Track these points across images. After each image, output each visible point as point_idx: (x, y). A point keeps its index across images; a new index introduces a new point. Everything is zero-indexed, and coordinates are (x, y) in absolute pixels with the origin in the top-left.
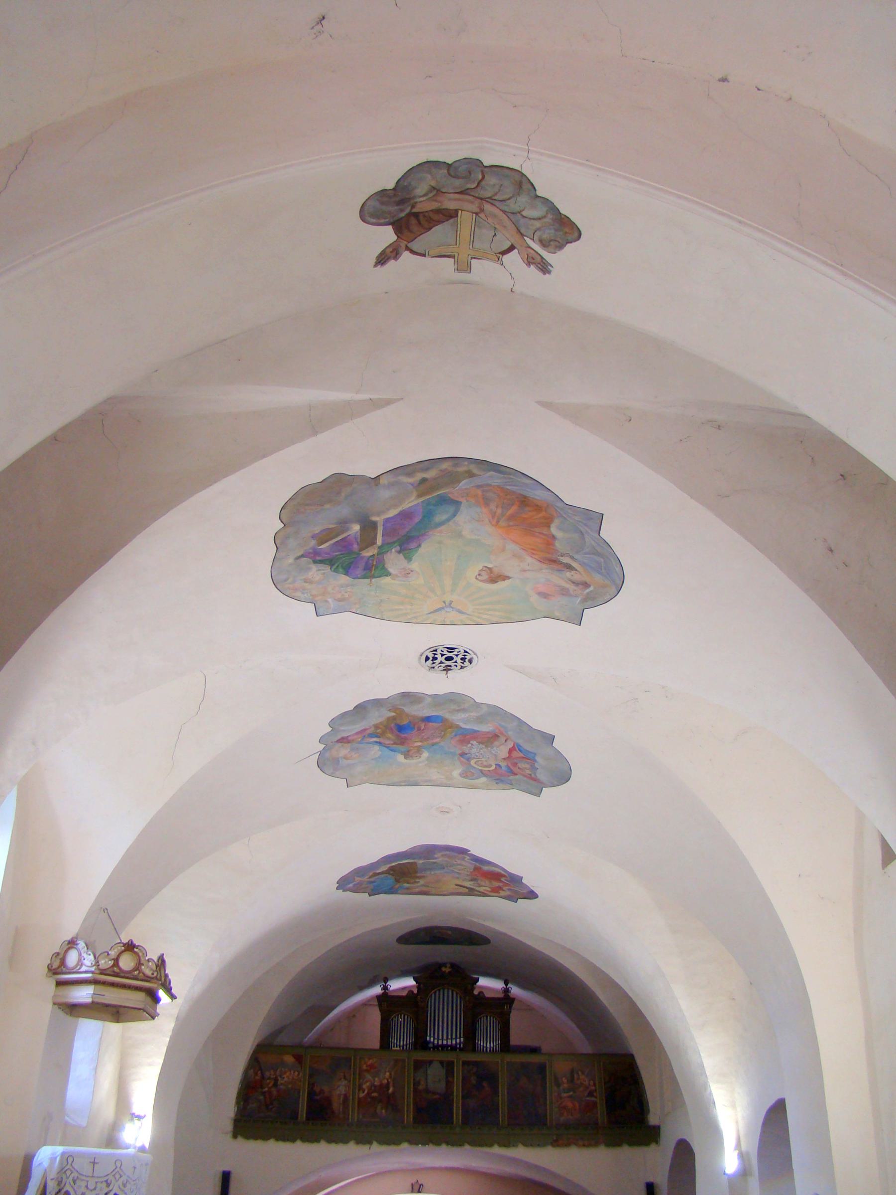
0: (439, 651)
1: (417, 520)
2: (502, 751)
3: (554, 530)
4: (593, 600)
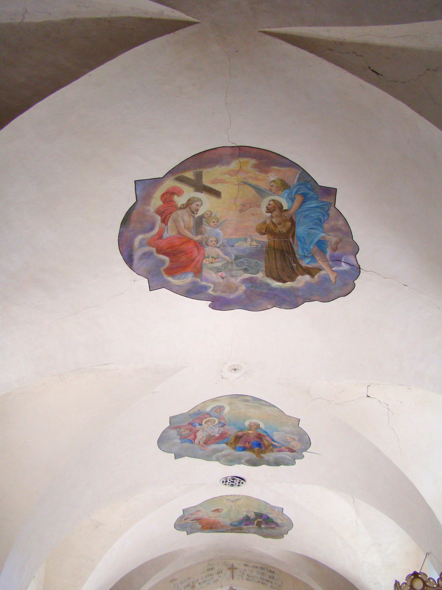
0: (237, 485)
1: (243, 523)
2: (201, 435)
3: (200, 526)
4: (181, 518)
